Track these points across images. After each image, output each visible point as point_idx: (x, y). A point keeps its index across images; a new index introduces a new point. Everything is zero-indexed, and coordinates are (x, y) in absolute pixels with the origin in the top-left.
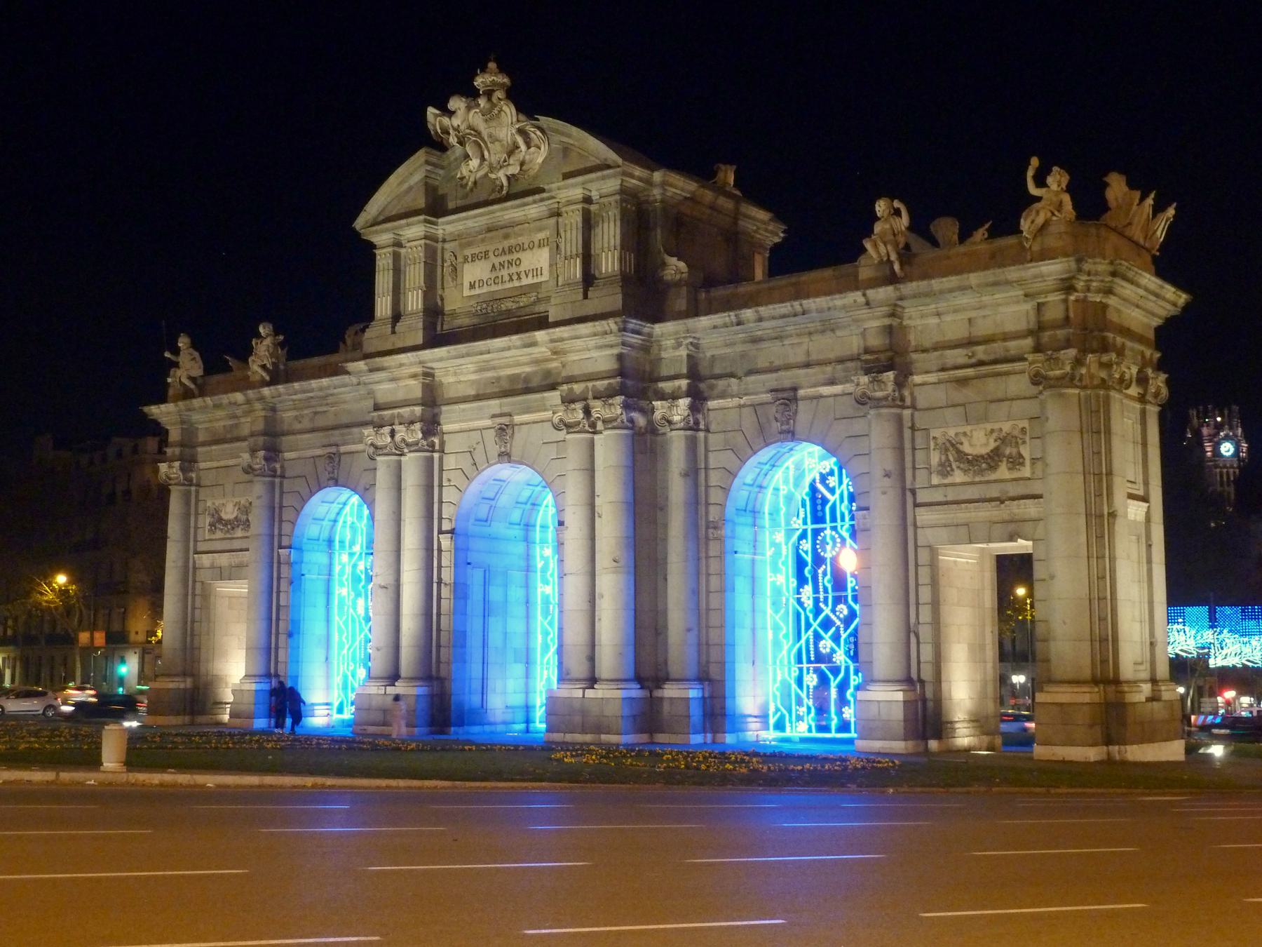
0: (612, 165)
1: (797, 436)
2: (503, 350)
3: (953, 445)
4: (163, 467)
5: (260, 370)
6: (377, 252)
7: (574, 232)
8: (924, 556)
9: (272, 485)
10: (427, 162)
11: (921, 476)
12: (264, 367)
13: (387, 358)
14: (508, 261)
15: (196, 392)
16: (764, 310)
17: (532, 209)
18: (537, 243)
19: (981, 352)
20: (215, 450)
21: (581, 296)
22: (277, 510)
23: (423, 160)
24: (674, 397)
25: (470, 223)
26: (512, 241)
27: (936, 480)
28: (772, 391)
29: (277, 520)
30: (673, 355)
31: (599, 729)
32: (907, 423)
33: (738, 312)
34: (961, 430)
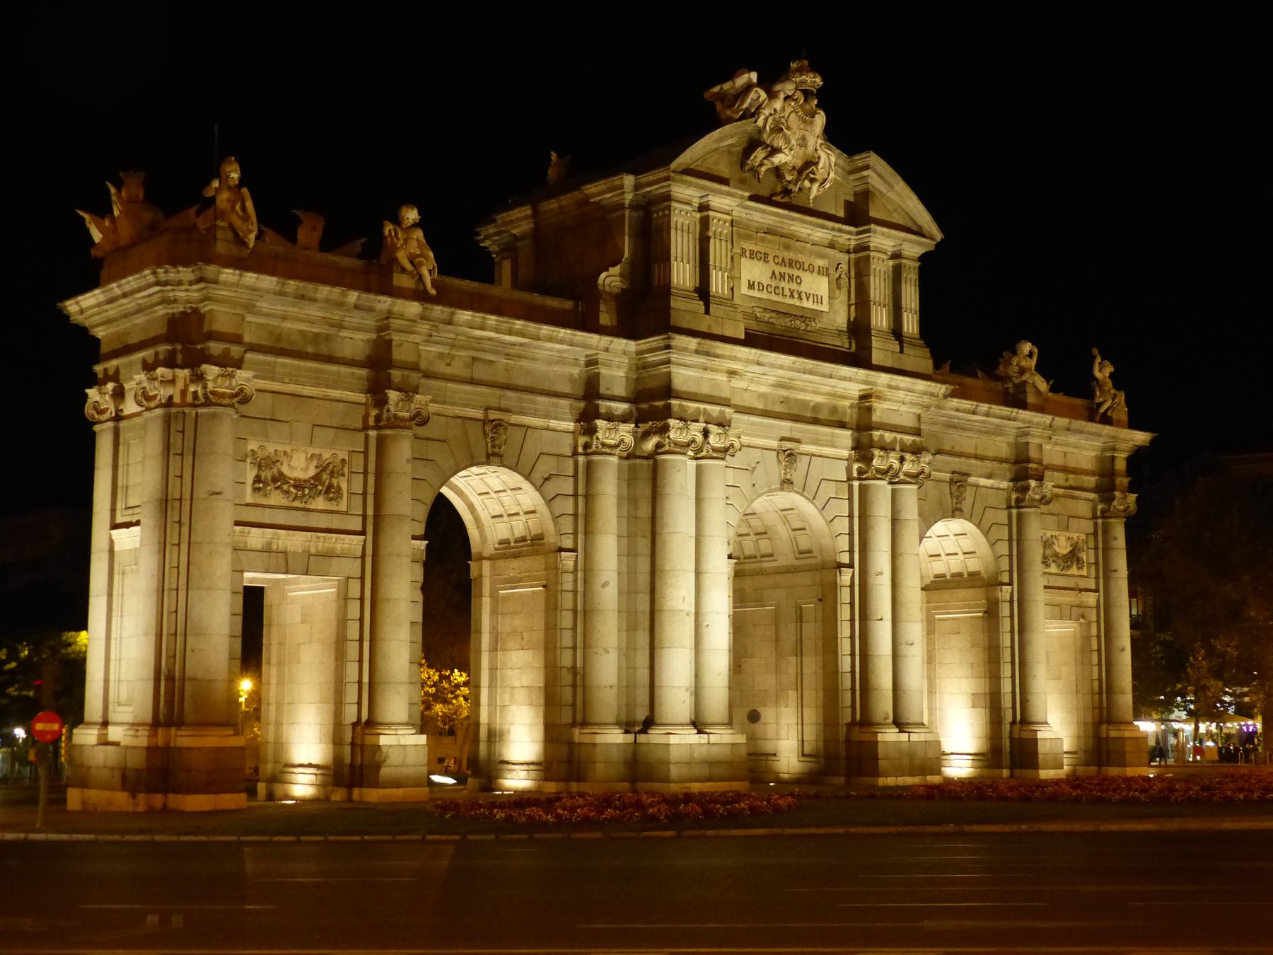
0: (927, 235)
2: (844, 379)
7: (882, 280)
14: (789, 275)
18: (816, 269)
20: (283, 365)
21: (898, 350)
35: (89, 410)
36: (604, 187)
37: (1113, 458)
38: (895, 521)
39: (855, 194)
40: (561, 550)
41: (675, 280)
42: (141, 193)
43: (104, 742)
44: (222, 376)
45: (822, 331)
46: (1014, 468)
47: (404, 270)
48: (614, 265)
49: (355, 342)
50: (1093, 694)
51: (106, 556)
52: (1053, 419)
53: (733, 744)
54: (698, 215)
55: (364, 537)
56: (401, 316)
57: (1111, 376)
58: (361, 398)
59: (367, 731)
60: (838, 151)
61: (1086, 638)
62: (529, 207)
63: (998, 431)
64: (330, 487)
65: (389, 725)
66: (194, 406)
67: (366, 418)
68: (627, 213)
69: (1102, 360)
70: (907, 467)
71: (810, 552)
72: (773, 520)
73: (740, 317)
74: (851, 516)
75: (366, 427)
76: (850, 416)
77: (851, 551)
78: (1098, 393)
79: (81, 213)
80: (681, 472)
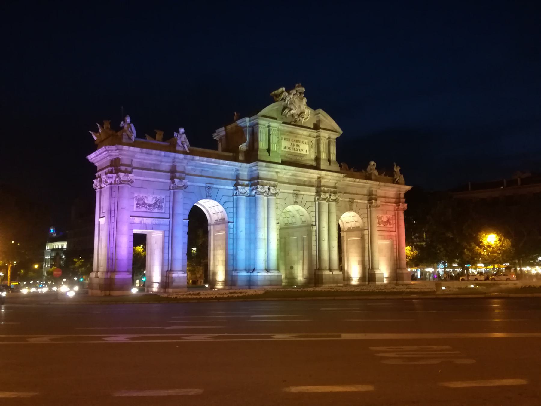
2: (311, 173)
18: (305, 143)
19: (387, 200)
21: (329, 164)
26: (297, 139)
35: (94, 186)
36: (241, 121)
37: (400, 194)
38: (329, 213)
39: (317, 121)
40: (229, 222)
41: (260, 146)
42: (109, 127)
43: (97, 277)
44: (124, 176)
45: (306, 160)
46: (369, 197)
47: (179, 146)
48: (244, 143)
49: (166, 165)
50: (394, 260)
51: (98, 226)
52: (379, 183)
54: (268, 128)
55: (169, 220)
56: (178, 158)
57: (400, 170)
58: (169, 181)
59: (170, 273)
60: (311, 109)
61: (392, 245)
62: (224, 127)
63: (363, 187)
64: (159, 206)
66: (118, 184)
67: (170, 187)
68: (248, 128)
69: (397, 166)
70: (332, 197)
71: (305, 222)
72: (295, 213)
73: (280, 156)
74: (316, 211)
75: (170, 189)
76: (316, 184)
77: (316, 221)
78: (395, 175)
79: (90, 132)
80: (263, 200)
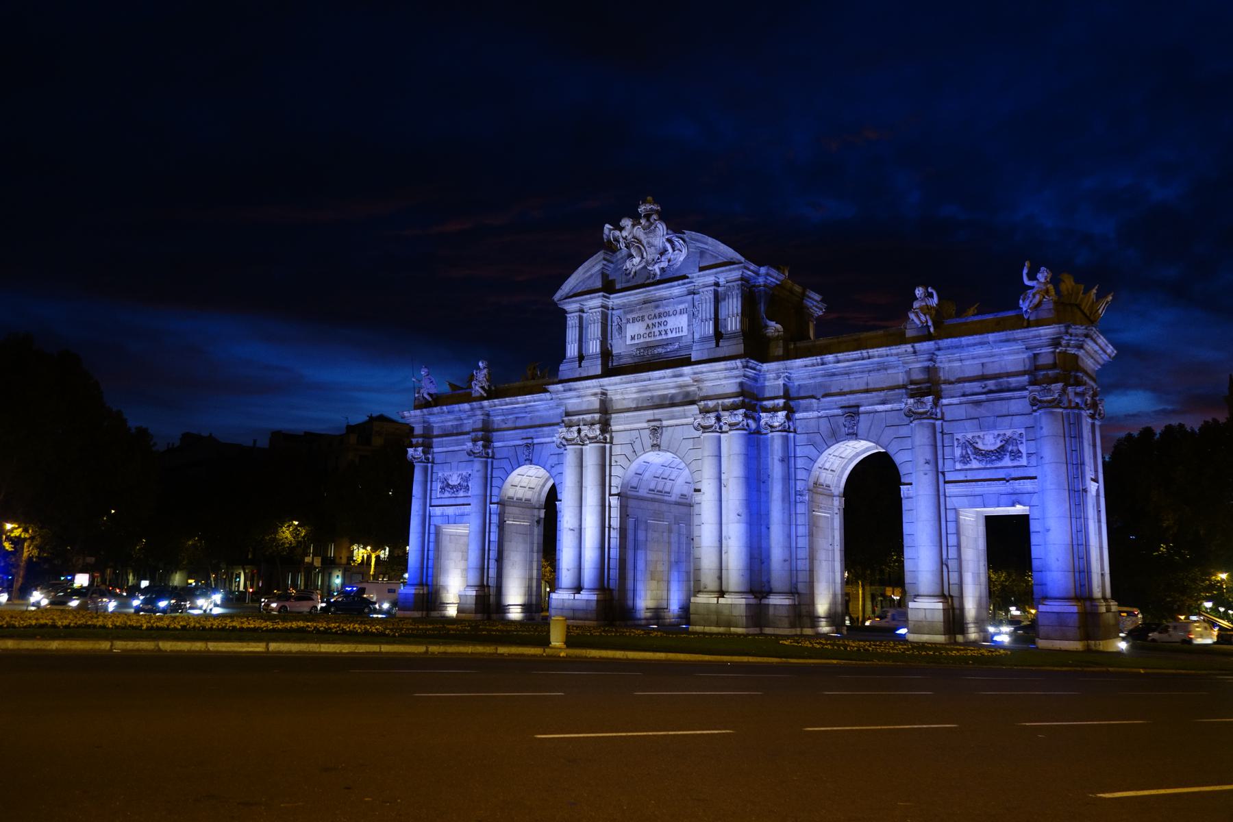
0: (737, 262)
1: (859, 437)
2: (660, 378)
3: (971, 444)
4: (411, 451)
5: (480, 390)
6: (568, 315)
7: (708, 304)
8: (951, 515)
9: (486, 463)
10: (604, 259)
11: (948, 463)
12: (483, 388)
13: (578, 383)
15: (433, 403)
16: (841, 356)
17: (677, 290)
18: (678, 311)
19: (991, 384)
20: (445, 440)
21: (714, 345)
22: (489, 479)
23: (602, 257)
24: (775, 410)
25: (632, 298)
26: (661, 310)
27: (958, 466)
28: (842, 407)
29: (489, 485)
30: (773, 383)
31: (729, 625)
32: (939, 429)
33: (822, 357)
34: (976, 434)
53: (587, 600)
65: (561, 588)
